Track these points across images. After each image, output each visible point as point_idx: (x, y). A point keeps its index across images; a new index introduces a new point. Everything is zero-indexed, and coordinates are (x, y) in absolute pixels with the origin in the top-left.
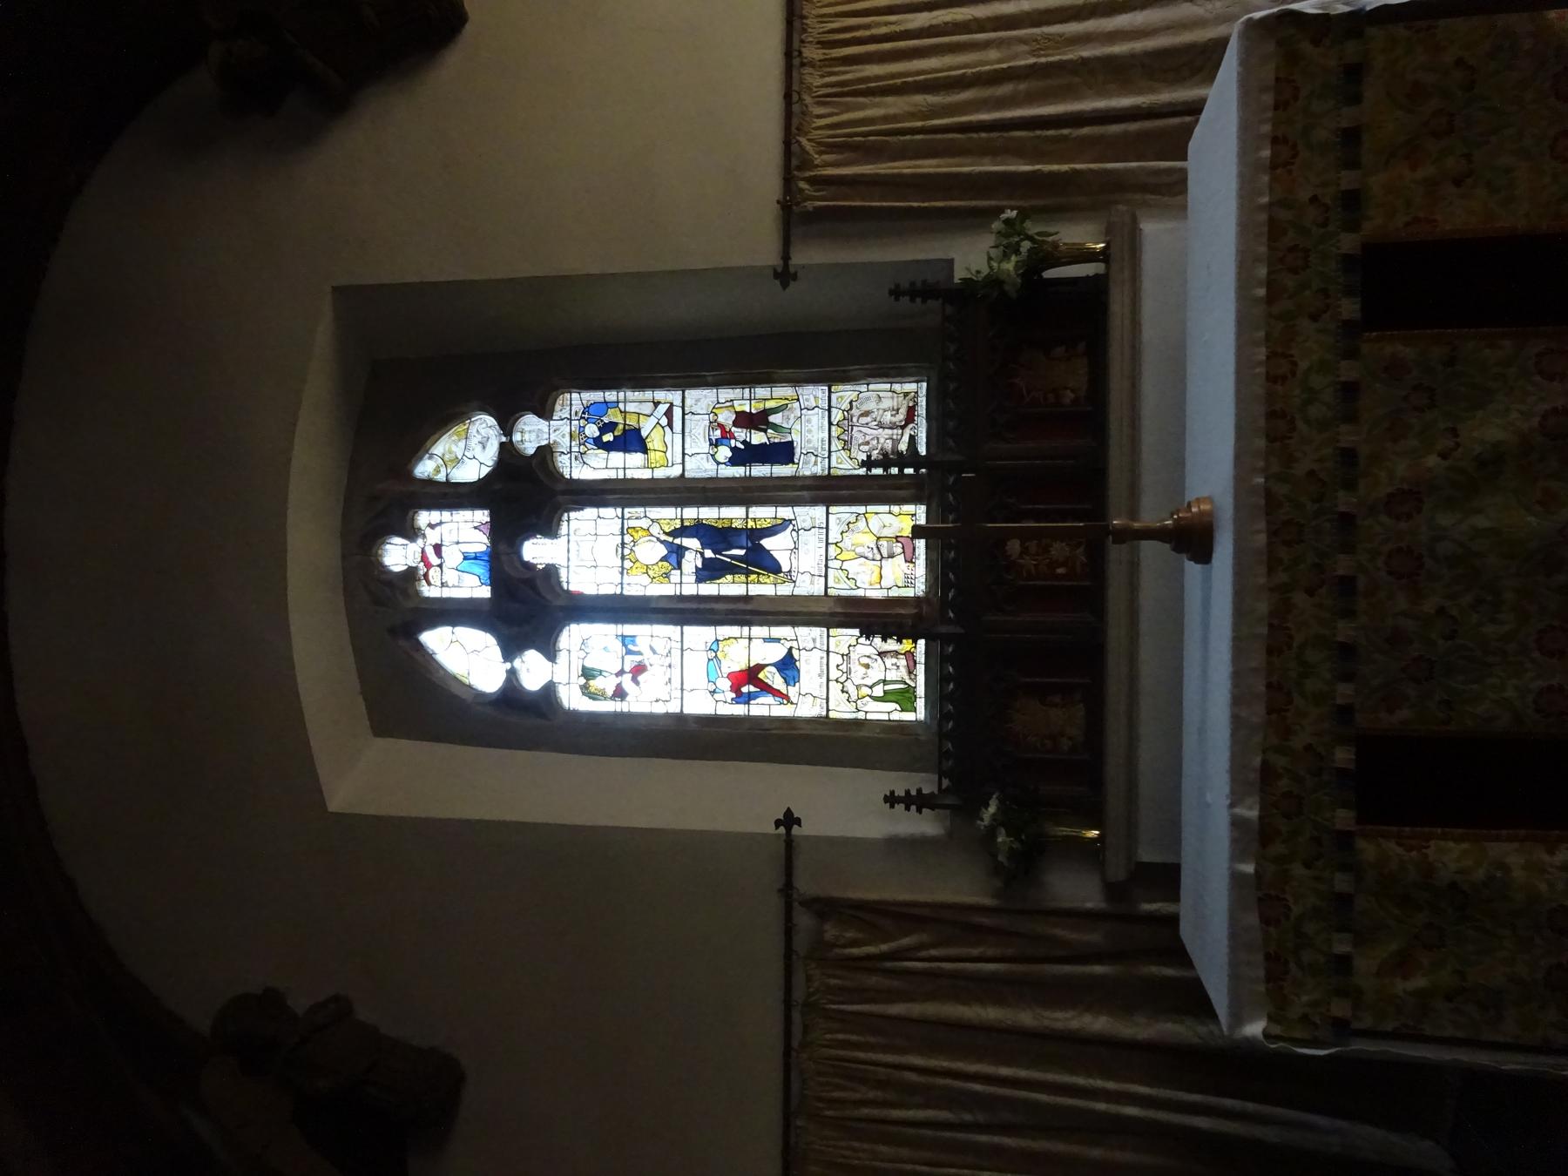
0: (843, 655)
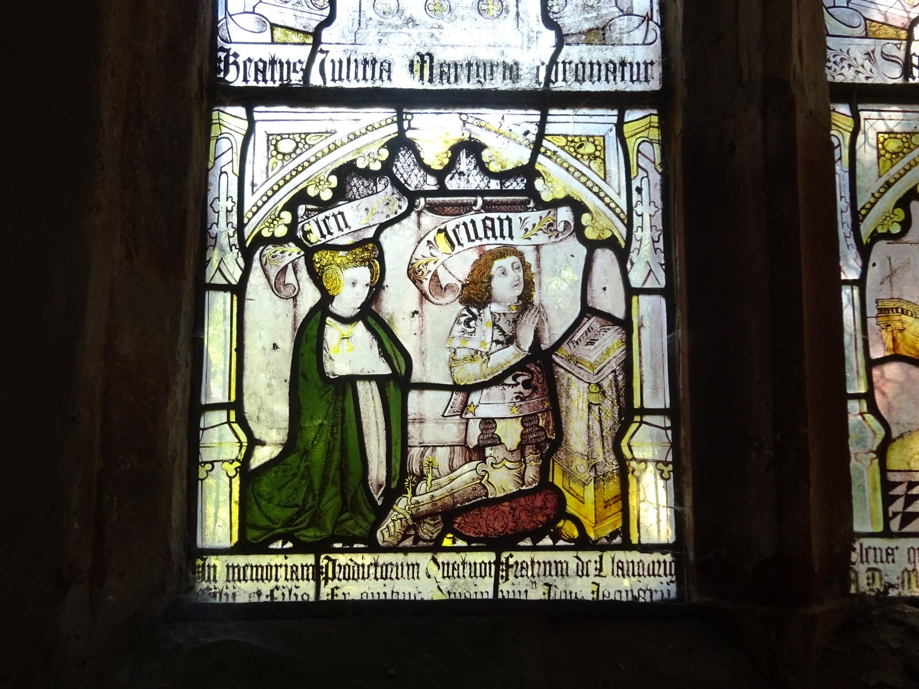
0: (529, 172)
